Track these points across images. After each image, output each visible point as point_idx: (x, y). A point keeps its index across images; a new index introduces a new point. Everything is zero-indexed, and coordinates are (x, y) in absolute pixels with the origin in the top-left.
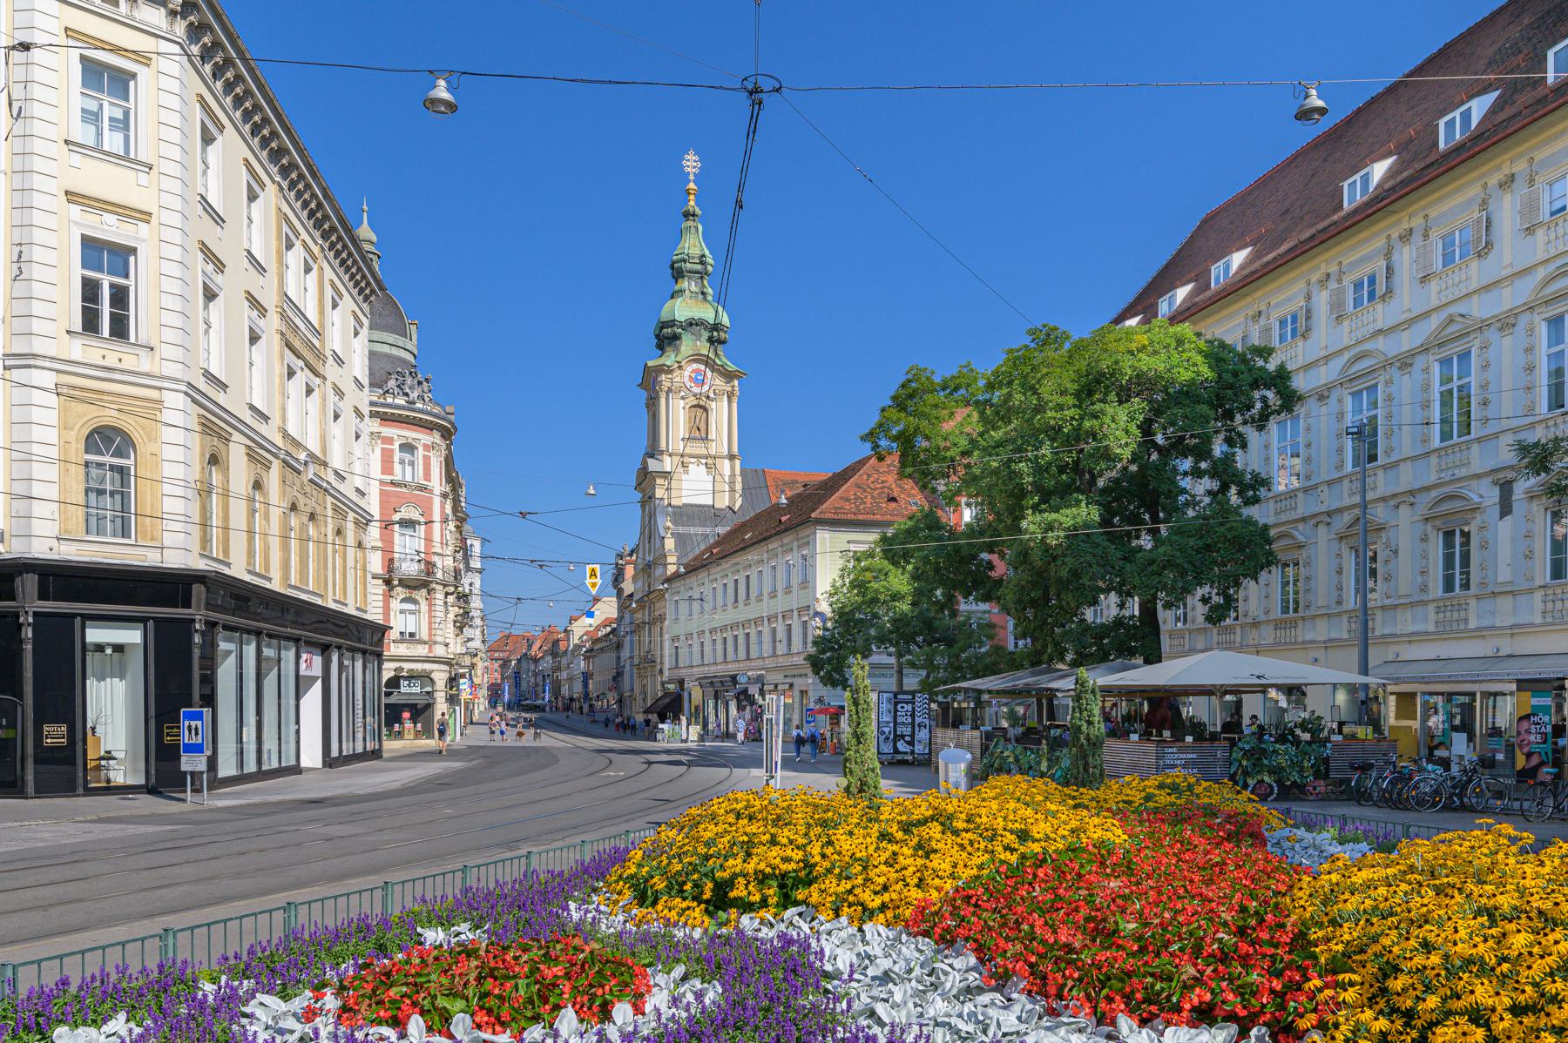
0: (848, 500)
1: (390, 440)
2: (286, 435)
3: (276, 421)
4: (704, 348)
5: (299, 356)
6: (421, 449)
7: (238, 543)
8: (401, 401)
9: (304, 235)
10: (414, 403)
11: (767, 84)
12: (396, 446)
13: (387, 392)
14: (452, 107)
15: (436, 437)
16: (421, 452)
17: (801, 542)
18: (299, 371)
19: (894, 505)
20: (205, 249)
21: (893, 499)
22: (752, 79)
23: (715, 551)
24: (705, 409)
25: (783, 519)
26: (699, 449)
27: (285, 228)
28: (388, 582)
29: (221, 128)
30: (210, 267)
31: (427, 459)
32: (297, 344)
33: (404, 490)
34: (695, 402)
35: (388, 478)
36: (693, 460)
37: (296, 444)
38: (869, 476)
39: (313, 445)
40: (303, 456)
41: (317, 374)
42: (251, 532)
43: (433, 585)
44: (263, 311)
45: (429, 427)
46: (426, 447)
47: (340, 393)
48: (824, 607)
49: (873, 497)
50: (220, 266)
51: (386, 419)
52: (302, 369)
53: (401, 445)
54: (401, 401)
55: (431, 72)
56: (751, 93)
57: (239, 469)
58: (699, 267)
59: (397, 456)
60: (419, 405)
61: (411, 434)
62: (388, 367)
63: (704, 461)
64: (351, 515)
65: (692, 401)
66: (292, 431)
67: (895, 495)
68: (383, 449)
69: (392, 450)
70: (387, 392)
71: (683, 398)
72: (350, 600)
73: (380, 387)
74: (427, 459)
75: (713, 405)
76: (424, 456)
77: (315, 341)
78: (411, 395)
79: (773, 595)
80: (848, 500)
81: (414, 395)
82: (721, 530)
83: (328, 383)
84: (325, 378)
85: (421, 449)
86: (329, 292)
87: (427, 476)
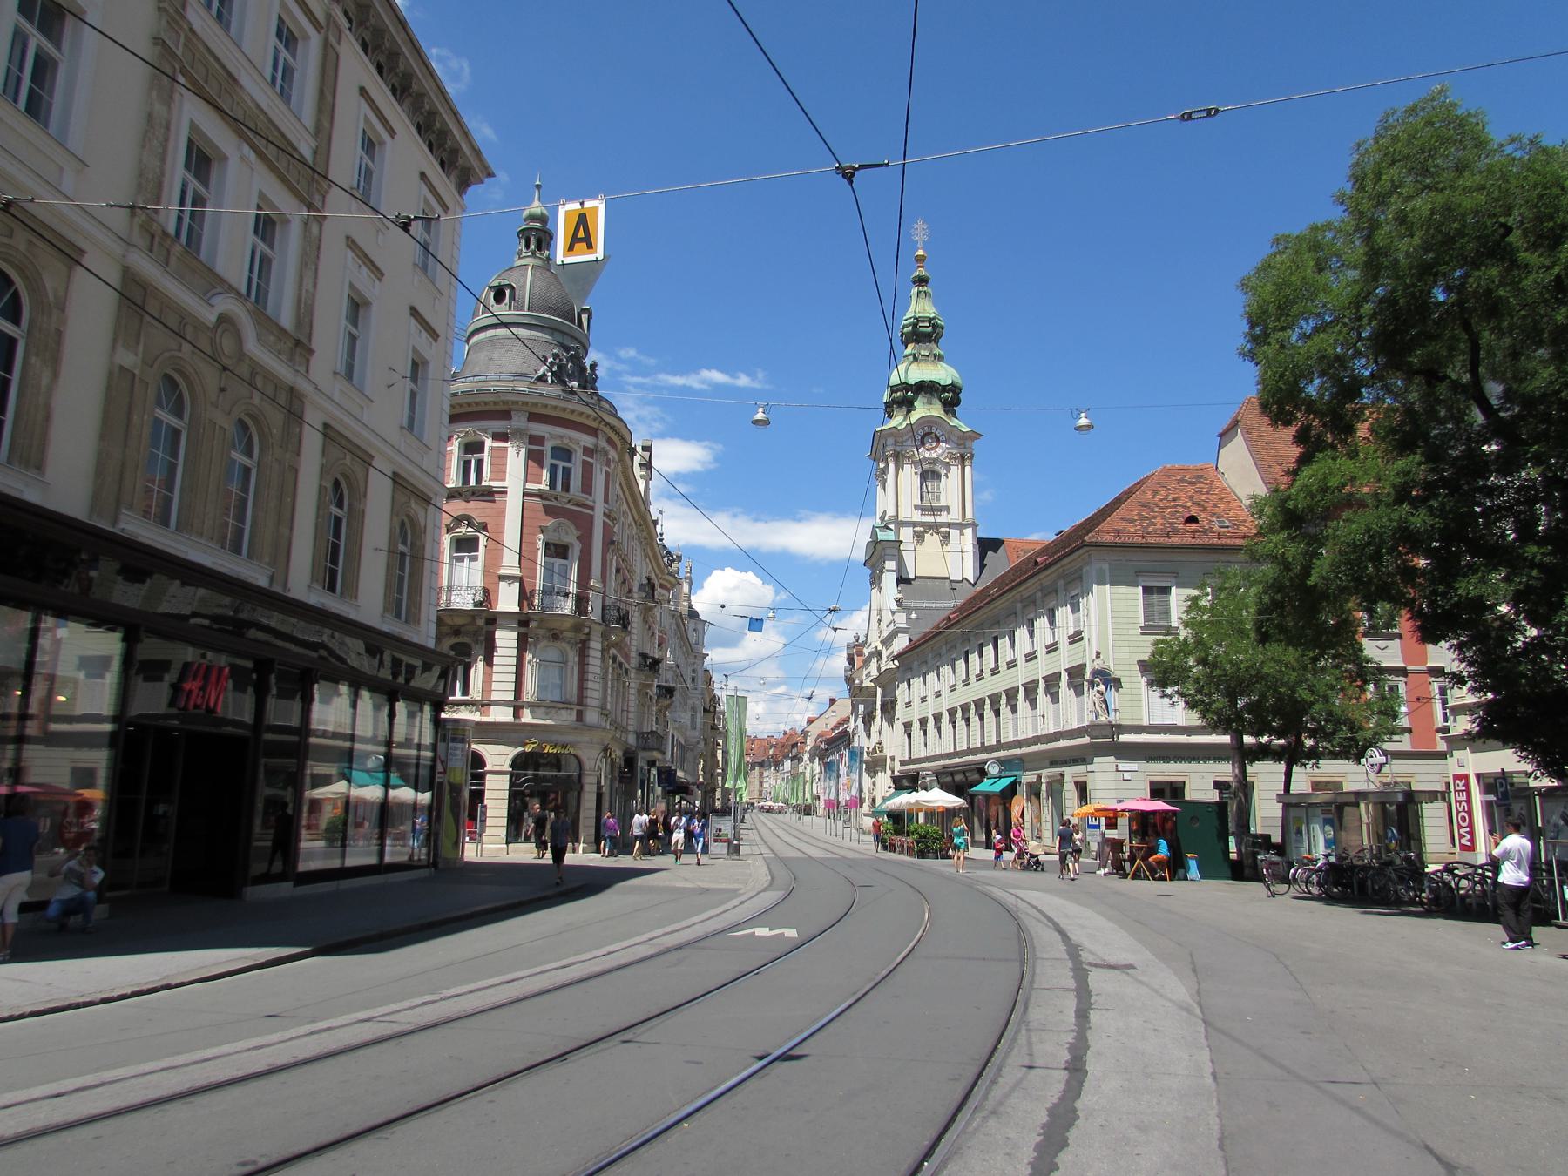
4: (937, 411)
6: (580, 451)
12: (547, 448)
16: (579, 457)
19: (1194, 526)
25: (1039, 560)
29: (392, 133)
31: (588, 470)
38: (1155, 493)
46: (588, 451)
49: (1164, 518)
58: (930, 329)
67: (1193, 513)
74: (588, 470)
76: (584, 462)
80: (1133, 521)
87: (587, 487)
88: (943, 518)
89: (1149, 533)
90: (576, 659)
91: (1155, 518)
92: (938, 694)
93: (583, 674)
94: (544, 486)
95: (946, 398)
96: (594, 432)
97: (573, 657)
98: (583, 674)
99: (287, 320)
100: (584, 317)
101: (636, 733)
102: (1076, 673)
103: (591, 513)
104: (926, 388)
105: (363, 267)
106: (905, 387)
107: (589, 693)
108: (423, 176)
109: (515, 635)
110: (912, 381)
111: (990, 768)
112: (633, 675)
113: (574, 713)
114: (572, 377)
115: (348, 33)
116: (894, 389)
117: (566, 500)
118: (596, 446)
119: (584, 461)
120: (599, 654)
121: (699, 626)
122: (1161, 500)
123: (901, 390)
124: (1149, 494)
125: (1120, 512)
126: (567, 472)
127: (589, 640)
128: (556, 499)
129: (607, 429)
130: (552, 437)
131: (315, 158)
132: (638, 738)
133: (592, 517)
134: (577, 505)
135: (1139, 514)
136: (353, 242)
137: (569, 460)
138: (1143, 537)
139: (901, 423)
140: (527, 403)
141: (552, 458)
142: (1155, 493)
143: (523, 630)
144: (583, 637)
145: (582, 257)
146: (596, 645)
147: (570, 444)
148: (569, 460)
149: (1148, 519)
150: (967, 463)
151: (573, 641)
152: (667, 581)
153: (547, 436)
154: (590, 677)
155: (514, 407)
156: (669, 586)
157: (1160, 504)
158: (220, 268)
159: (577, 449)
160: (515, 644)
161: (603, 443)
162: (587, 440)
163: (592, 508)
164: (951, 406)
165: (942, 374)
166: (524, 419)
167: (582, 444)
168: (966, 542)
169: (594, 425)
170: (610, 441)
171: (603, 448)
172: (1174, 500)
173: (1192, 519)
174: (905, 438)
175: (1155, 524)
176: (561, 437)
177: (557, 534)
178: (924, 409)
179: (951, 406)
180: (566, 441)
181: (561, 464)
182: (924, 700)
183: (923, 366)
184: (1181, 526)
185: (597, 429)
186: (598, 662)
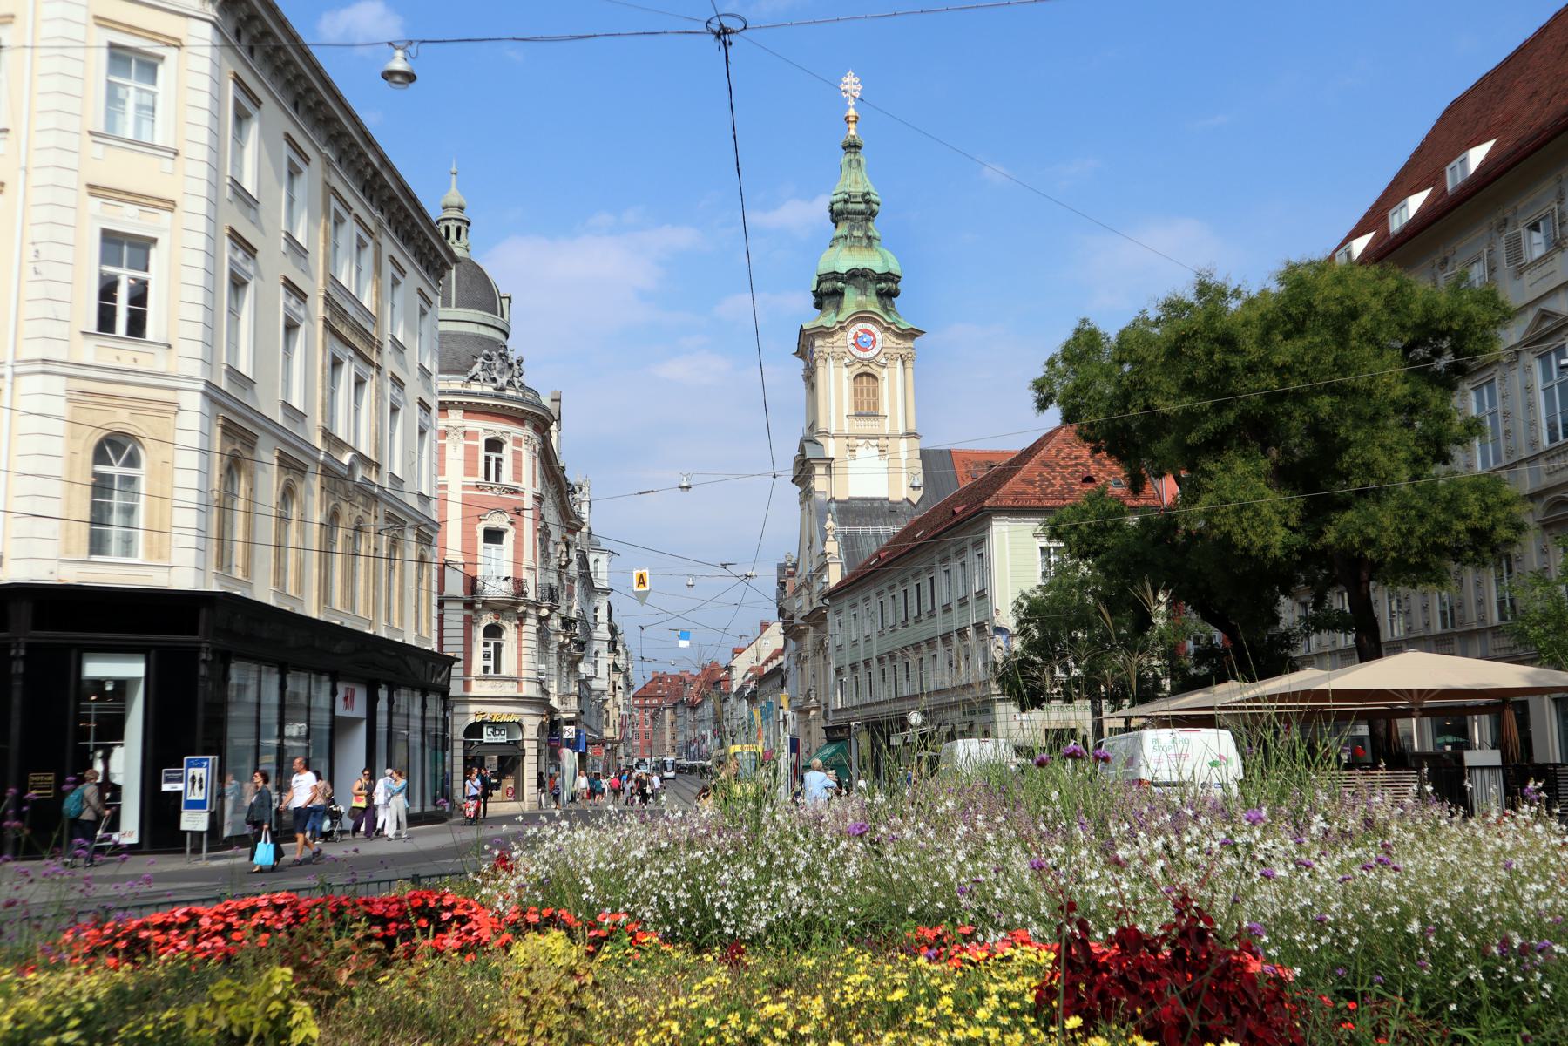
0: (1032, 483)
1: (475, 435)
2: (328, 435)
3: (316, 420)
4: (873, 305)
5: (348, 344)
7: (265, 558)
9: (357, 208)
11: (729, 23)
12: (481, 443)
13: (472, 378)
14: (409, 77)
15: (526, 431)
16: (508, 449)
18: (346, 363)
20: (235, 236)
21: (1089, 479)
22: (716, 21)
23: (882, 555)
25: (957, 510)
27: (334, 203)
28: (469, 605)
30: (240, 255)
32: (344, 331)
33: (490, 493)
34: (862, 370)
35: (472, 480)
36: (861, 442)
37: (341, 445)
38: (1059, 451)
39: (365, 448)
40: (346, 459)
41: (370, 363)
42: (280, 546)
43: (522, 609)
44: (302, 296)
45: (517, 418)
47: (398, 383)
48: (1009, 621)
49: (1063, 478)
50: (251, 251)
51: (471, 410)
52: (351, 359)
54: (489, 389)
55: (390, 44)
56: (718, 36)
57: (270, 480)
58: (862, 207)
60: (510, 392)
61: (497, 428)
62: (474, 350)
63: (874, 442)
64: (410, 523)
65: (857, 369)
66: (341, 433)
67: (1092, 473)
68: (467, 446)
69: (476, 447)
70: (472, 378)
71: (847, 366)
72: (360, 611)
73: (465, 373)
74: (517, 456)
75: (885, 372)
77: (369, 327)
80: (1032, 483)
81: (502, 381)
82: (895, 529)
86: (388, 268)
87: (517, 475)
88: (886, 427)
89: (1046, 495)
91: (1054, 478)
92: (868, 639)
94: (481, 478)
95: (882, 289)
100: (505, 302)
104: (855, 276)
106: (835, 276)
108: (420, 290)
109: (461, 618)
110: (843, 267)
115: (386, 227)
116: (822, 279)
122: (1064, 459)
123: (831, 280)
124: (1054, 452)
125: (1023, 472)
126: (498, 460)
135: (1040, 475)
138: (1040, 500)
141: (487, 449)
142: (1059, 451)
143: (467, 612)
145: (642, 589)
149: (1049, 480)
150: (909, 364)
157: (1062, 463)
160: (461, 625)
164: (887, 296)
165: (875, 261)
168: (906, 451)
169: (522, 416)
172: (1076, 458)
173: (1089, 479)
174: (835, 338)
175: (1053, 485)
178: (853, 300)
179: (887, 296)
180: (498, 435)
181: (493, 456)
182: (855, 643)
183: (855, 251)
184: (1077, 487)
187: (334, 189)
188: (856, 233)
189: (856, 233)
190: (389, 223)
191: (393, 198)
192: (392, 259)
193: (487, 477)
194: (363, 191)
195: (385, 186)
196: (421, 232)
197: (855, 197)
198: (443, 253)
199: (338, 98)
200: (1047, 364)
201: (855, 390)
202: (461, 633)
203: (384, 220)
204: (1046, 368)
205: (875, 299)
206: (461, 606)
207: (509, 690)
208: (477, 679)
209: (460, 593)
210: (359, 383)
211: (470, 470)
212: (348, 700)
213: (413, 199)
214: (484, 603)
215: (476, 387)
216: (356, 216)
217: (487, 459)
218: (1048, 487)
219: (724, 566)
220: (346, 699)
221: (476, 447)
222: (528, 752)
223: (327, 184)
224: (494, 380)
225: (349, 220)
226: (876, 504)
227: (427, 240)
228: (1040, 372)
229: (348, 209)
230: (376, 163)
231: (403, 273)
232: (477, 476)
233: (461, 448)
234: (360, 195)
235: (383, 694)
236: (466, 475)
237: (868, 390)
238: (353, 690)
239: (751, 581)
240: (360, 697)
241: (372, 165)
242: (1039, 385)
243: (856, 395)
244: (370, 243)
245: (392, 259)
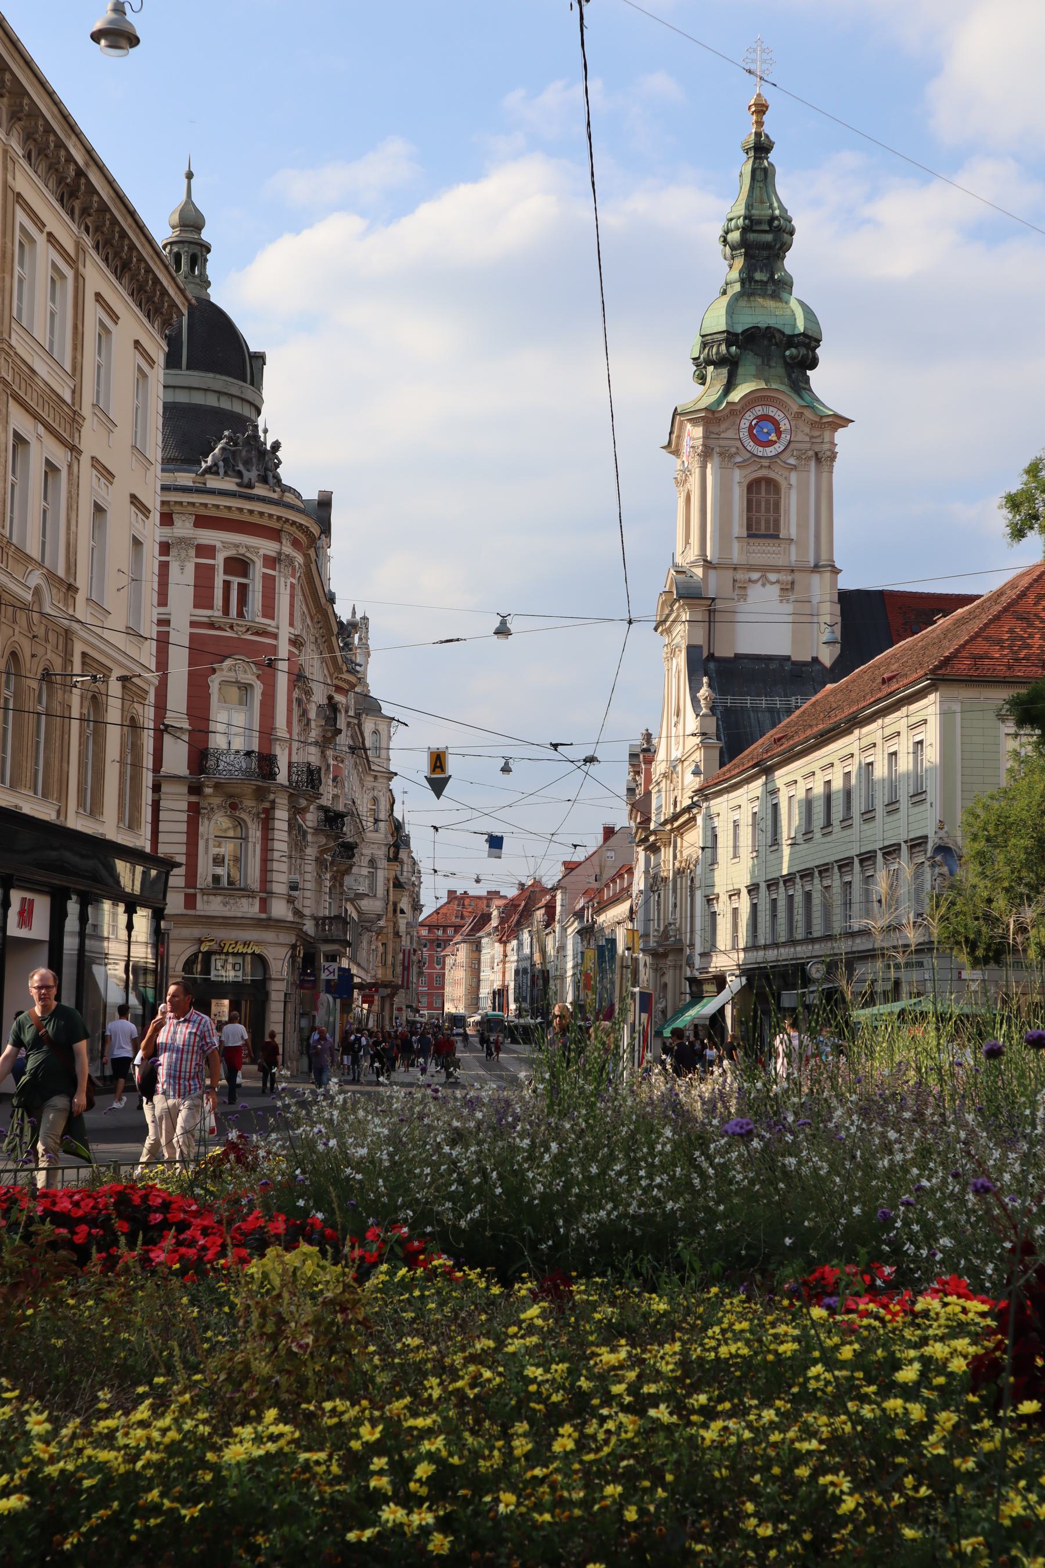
0: (1000, 642)
1: (207, 551)
6: (259, 563)
8: (229, 484)
10: (250, 486)
16: (258, 570)
17: (913, 720)
24: (772, 485)
26: (764, 553)
31: (269, 582)
36: (755, 576)
46: (271, 562)
53: (227, 560)
58: (769, 237)
59: (220, 578)
60: (260, 490)
63: (773, 577)
68: (198, 566)
69: (212, 567)
74: (269, 582)
75: (794, 477)
76: (265, 576)
78: (247, 475)
79: (868, 815)
80: (1000, 642)
83: (85, 460)
84: (80, 452)
85: (259, 563)
87: (269, 610)
90: (259, 834)
93: (266, 850)
94: (217, 613)
96: (274, 534)
97: (255, 833)
98: (266, 850)
99: (61, 573)
101: (315, 918)
102: (917, 844)
103: (274, 642)
105: (102, 480)
107: (276, 877)
108: (137, 343)
109: (184, 806)
111: (814, 970)
112: (309, 838)
113: (257, 902)
114: (247, 463)
115: (93, 253)
117: (244, 629)
118: (280, 553)
119: (265, 576)
120: (285, 826)
121: (382, 727)
126: (243, 589)
127: (273, 808)
128: (231, 627)
129: (293, 530)
130: (226, 545)
131: (73, 398)
132: (317, 925)
133: (275, 649)
134: (257, 634)
135: (1011, 631)
136: (98, 461)
137: (245, 575)
139: (719, 402)
140: (193, 504)
141: (226, 572)
143: (194, 799)
144: (267, 805)
146: (282, 814)
147: (248, 555)
148: (245, 575)
149: (1022, 638)
151: (254, 811)
152: (345, 680)
153: (219, 545)
154: (276, 855)
155: (177, 509)
156: (346, 686)
158: (28, 552)
159: (255, 558)
160: (184, 817)
161: (288, 549)
162: (268, 547)
163: (275, 636)
166: (189, 523)
167: (262, 552)
169: (277, 525)
170: (296, 544)
171: (288, 556)
174: (723, 426)
175: (1029, 647)
176: (237, 546)
177: (233, 674)
180: (242, 551)
181: (235, 580)
185: (280, 531)
186: (284, 836)
187: (19, 195)
188: (758, 276)
189: (758, 276)
190: (97, 247)
191: (104, 208)
192: (98, 296)
193: (226, 611)
194: (61, 200)
195: (92, 190)
196: (141, 259)
197: (759, 222)
198: (172, 291)
199: (28, 64)
200: (1028, 472)
201: (749, 502)
202: (184, 827)
203: (88, 241)
204: (1025, 477)
205: (780, 371)
206: (185, 790)
207: (250, 908)
208: (204, 892)
209: (183, 770)
210: (51, 468)
211: (202, 597)
212: (26, 917)
213: (132, 213)
214: (217, 786)
215: (213, 483)
216: (50, 234)
217: (227, 585)
218: (1021, 648)
219: (555, 746)
220: (21, 913)
221: (212, 567)
222: (274, 996)
223: (6, 186)
224: (240, 475)
225: (41, 239)
226: (773, 666)
227: (149, 270)
228: (1016, 484)
229: (40, 225)
230: (79, 157)
231: (115, 318)
232: (211, 608)
233: (190, 568)
234: (57, 205)
235: (73, 907)
236: (195, 606)
237: (768, 502)
238: (32, 902)
239: (592, 768)
240: (42, 906)
241: (76, 163)
242: (1014, 503)
243: (749, 509)
244: (69, 273)
245: (98, 296)
